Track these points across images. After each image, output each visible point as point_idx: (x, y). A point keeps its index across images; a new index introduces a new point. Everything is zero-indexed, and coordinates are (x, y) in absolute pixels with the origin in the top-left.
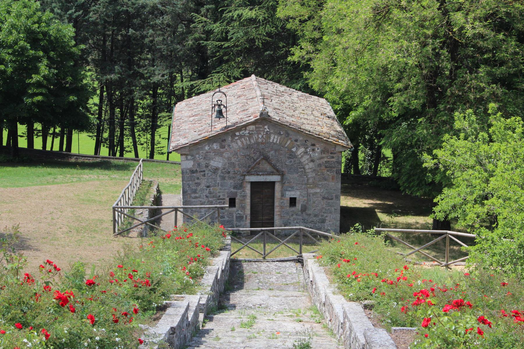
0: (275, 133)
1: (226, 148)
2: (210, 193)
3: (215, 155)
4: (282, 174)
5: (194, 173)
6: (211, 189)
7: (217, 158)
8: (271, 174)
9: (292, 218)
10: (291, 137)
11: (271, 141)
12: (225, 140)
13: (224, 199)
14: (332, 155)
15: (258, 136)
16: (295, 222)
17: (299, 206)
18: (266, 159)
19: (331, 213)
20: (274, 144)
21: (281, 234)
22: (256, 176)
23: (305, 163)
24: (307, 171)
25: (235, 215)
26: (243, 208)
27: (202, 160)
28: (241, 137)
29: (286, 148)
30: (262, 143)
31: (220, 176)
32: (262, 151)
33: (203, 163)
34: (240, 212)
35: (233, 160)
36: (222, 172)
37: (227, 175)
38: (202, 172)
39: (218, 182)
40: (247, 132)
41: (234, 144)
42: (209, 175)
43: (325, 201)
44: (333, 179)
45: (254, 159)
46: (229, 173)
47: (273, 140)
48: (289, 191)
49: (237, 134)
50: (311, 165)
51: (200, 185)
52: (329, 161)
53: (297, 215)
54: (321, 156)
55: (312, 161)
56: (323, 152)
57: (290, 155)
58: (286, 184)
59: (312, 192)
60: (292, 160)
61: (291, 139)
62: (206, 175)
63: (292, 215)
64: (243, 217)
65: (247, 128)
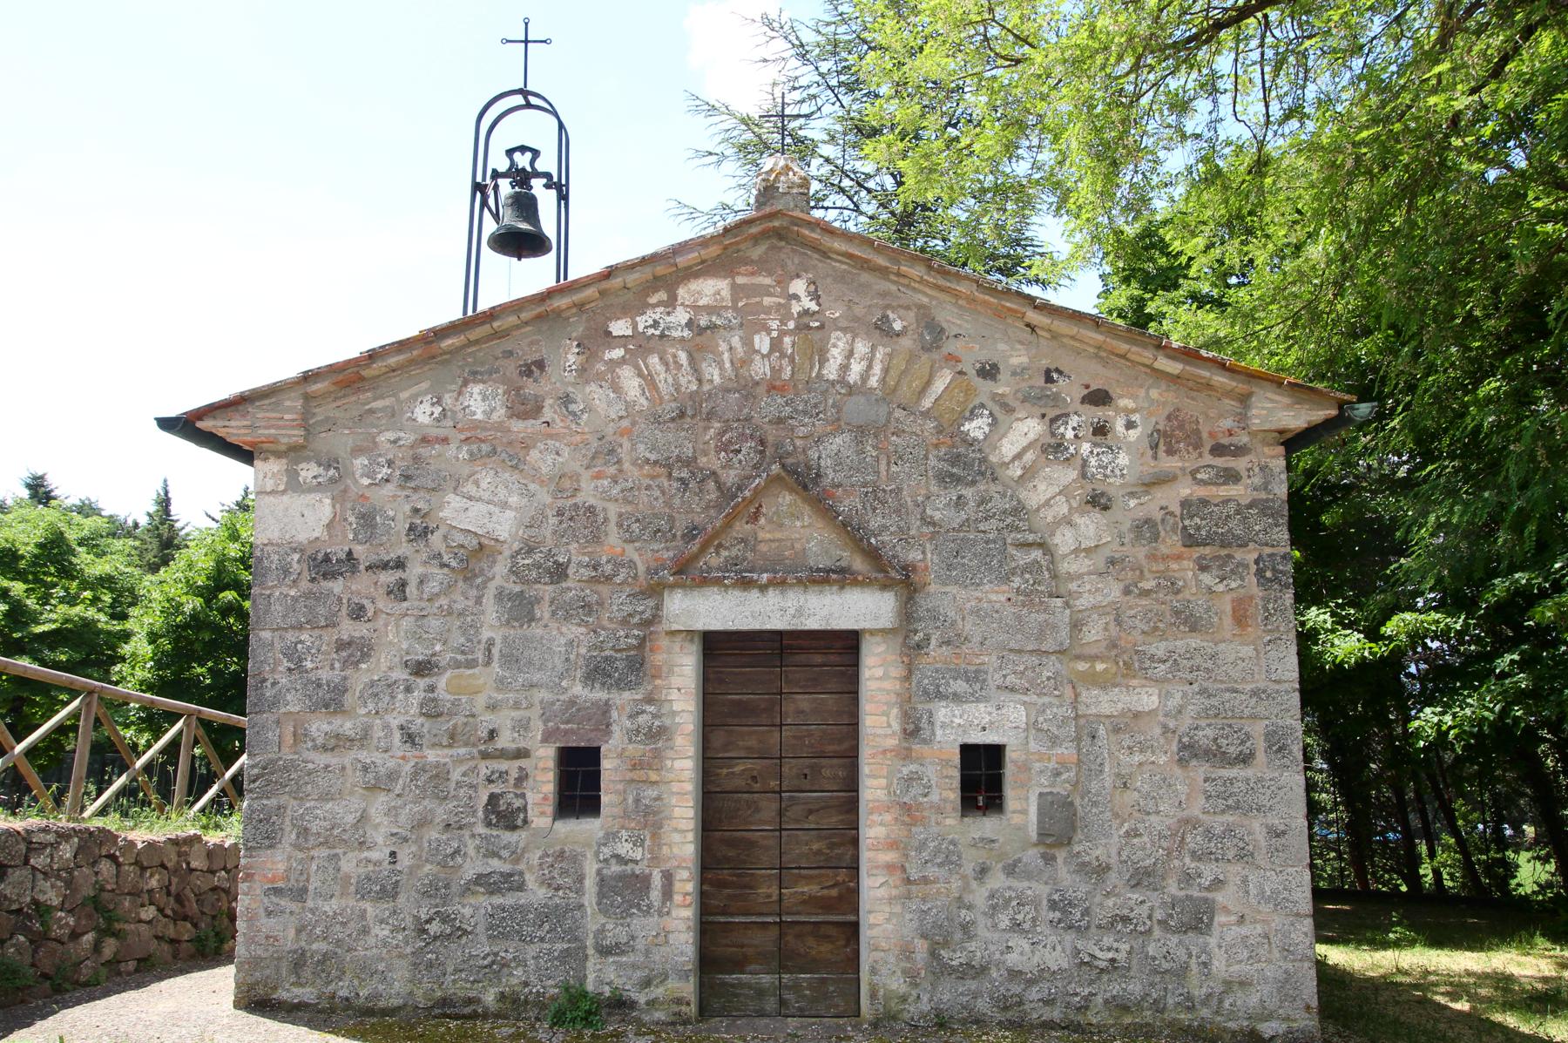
0: (852, 328)
1: (548, 414)
2: (432, 710)
3: (473, 457)
4: (906, 583)
5: (329, 575)
6: (442, 682)
7: (486, 479)
8: (835, 577)
9: (979, 896)
10: (951, 347)
11: (831, 371)
12: (540, 365)
13: (521, 754)
14: (1221, 462)
15: (748, 342)
16: (1004, 921)
17: (1023, 804)
18: (804, 480)
19: (1244, 856)
20: (852, 390)
21: (912, 1010)
22: (736, 595)
23: (1049, 515)
24: (1065, 567)
25: (590, 868)
26: (649, 819)
27: (389, 489)
28: (640, 345)
29: (926, 414)
30: (774, 387)
31: (500, 596)
32: (772, 434)
33: (396, 508)
34: (624, 849)
35: (588, 494)
36: (514, 571)
37: (547, 591)
38: (385, 566)
39: (486, 634)
40: (681, 316)
41: (597, 395)
42: (433, 587)
43: (1200, 770)
44: (1240, 619)
45: (720, 486)
46: (559, 573)
47: (845, 368)
48: (957, 698)
49: (619, 328)
50: (1090, 526)
51: (365, 656)
52: (1204, 502)
53: (1011, 870)
54: (1149, 467)
55: (1098, 502)
56: (1164, 440)
57: (955, 460)
58: (935, 651)
59: (1106, 708)
60: (968, 492)
61: (952, 358)
62: (411, 590)
63: (983, 872)
64: (644, 882)
65: (681, 292)
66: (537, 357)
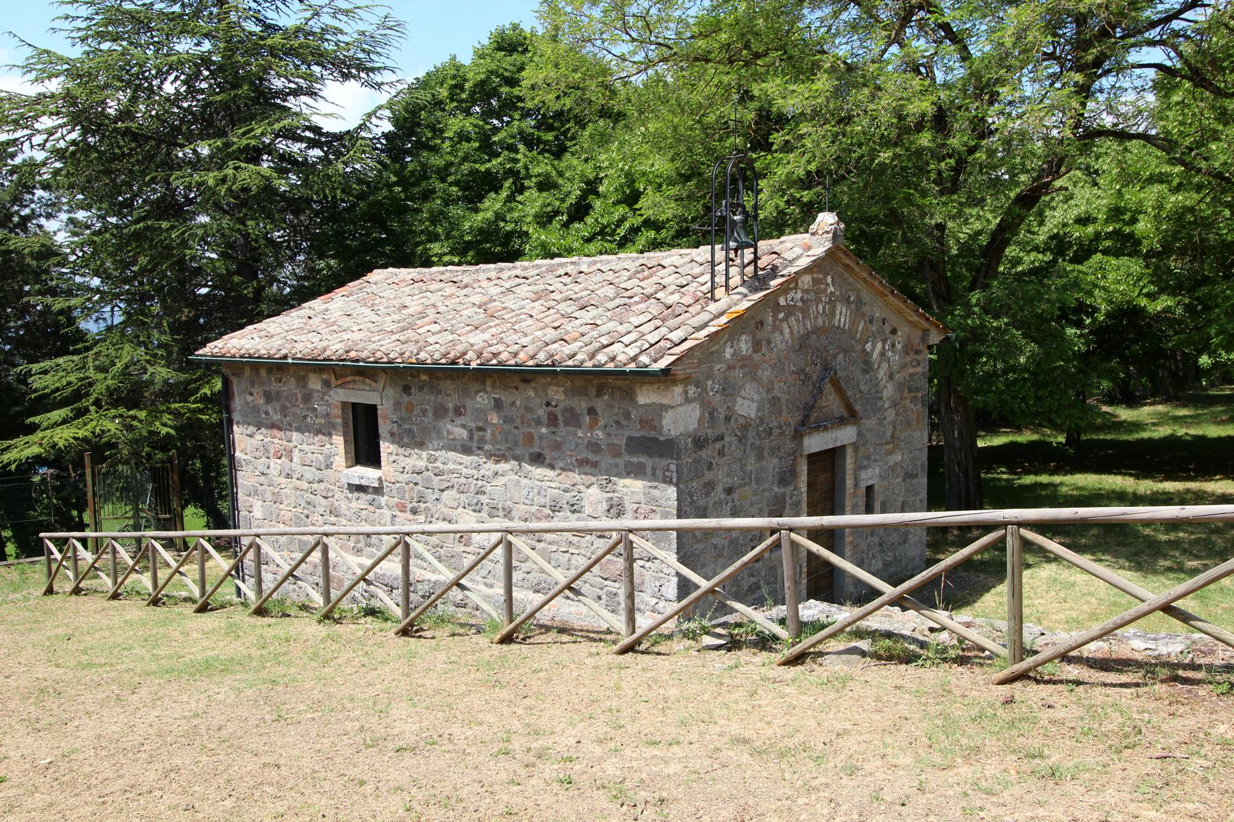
10: (866, 309)
35: (776, 393)
40: (799, 295)
42: (733, 447)
46: (769, 432)
66: (758, 319)
